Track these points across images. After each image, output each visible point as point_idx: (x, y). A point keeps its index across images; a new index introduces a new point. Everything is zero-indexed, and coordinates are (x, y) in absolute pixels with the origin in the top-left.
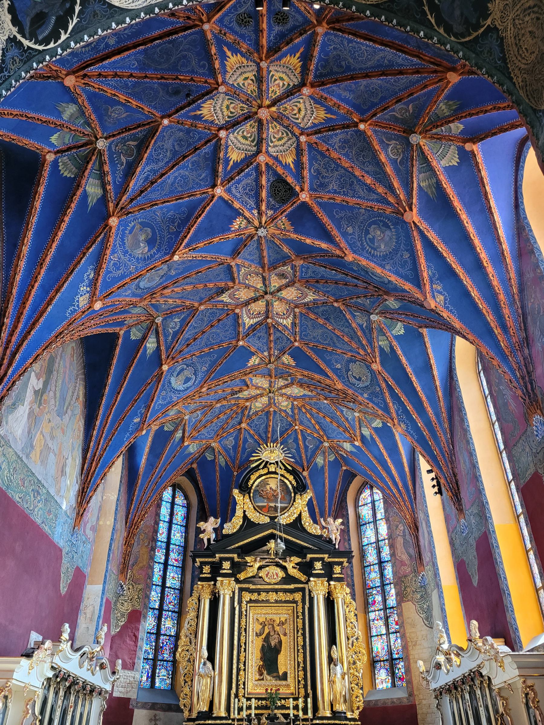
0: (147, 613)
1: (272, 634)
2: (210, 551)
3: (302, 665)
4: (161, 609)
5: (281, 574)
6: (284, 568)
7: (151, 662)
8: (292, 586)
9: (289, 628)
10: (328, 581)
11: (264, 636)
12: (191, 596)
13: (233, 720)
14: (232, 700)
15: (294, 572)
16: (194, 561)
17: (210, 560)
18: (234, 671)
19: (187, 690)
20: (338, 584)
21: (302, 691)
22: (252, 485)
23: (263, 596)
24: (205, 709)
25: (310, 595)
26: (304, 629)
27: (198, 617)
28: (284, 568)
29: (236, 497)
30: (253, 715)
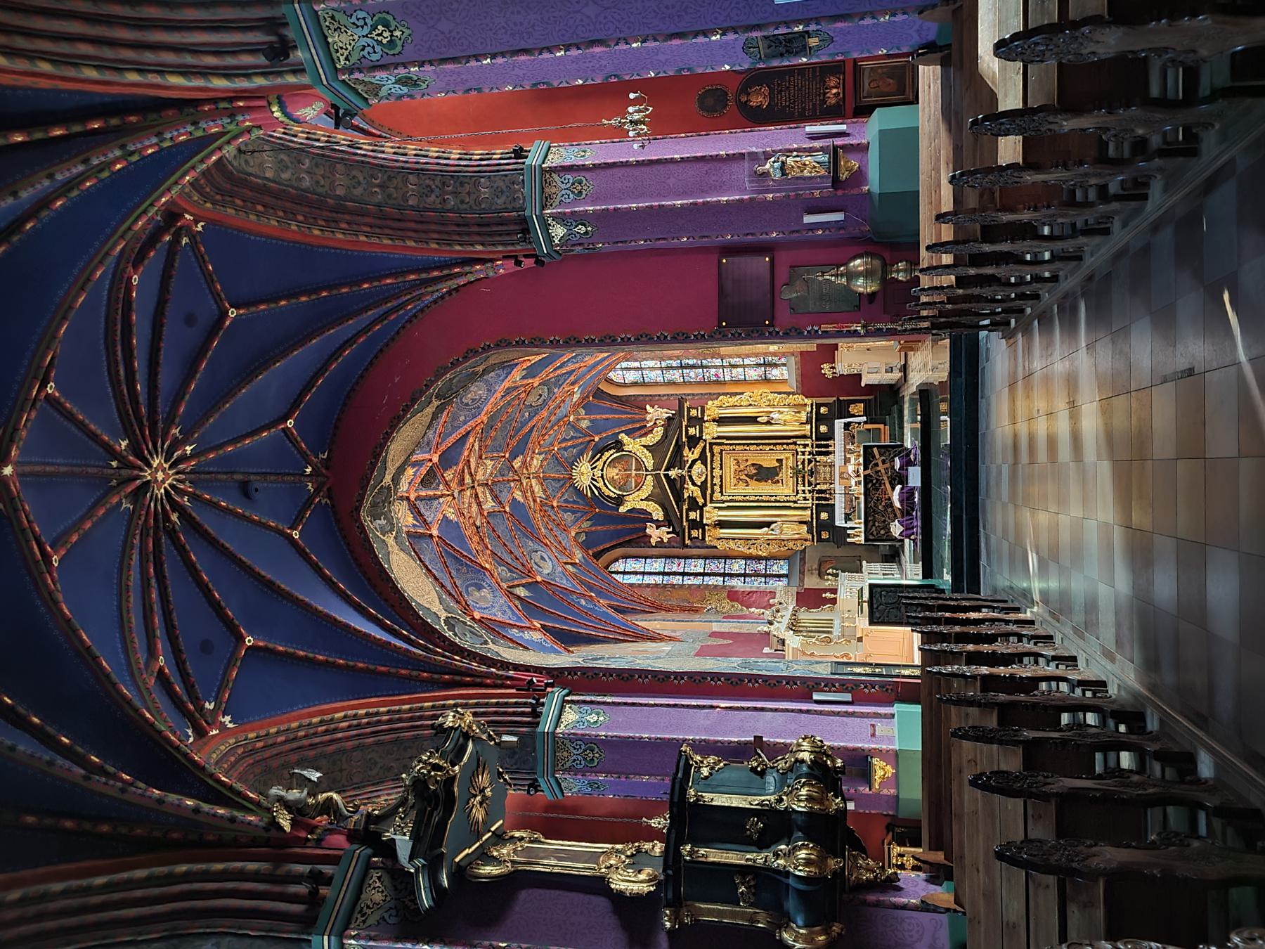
0: (729, 586)
1: (746, 472)
2: (678, 532)
3: (772, 447)
4: (724, 575)
5: (699, 464)
6: (694, 462)
7: (768, 579)
8: (709, 455)
9: (741, 457)
10: (705, 422)
11: (748, 480)
12: (716, 547)
13: (813, 504)
14: (798, 505)
15: (698, 450)
16: (687, 546)
17: (687, 531)
18: (777, 504)
19: (790, 544)
20: (707, 413)
21: (792, 447)
22: (615, 493)
23: (717, 481)
24: (805, 527)
25: (716, 439)
26: (744, 444)
27: (734, 539)
28: (694, 462)
29: (627, 509)
30: (809, 488)
